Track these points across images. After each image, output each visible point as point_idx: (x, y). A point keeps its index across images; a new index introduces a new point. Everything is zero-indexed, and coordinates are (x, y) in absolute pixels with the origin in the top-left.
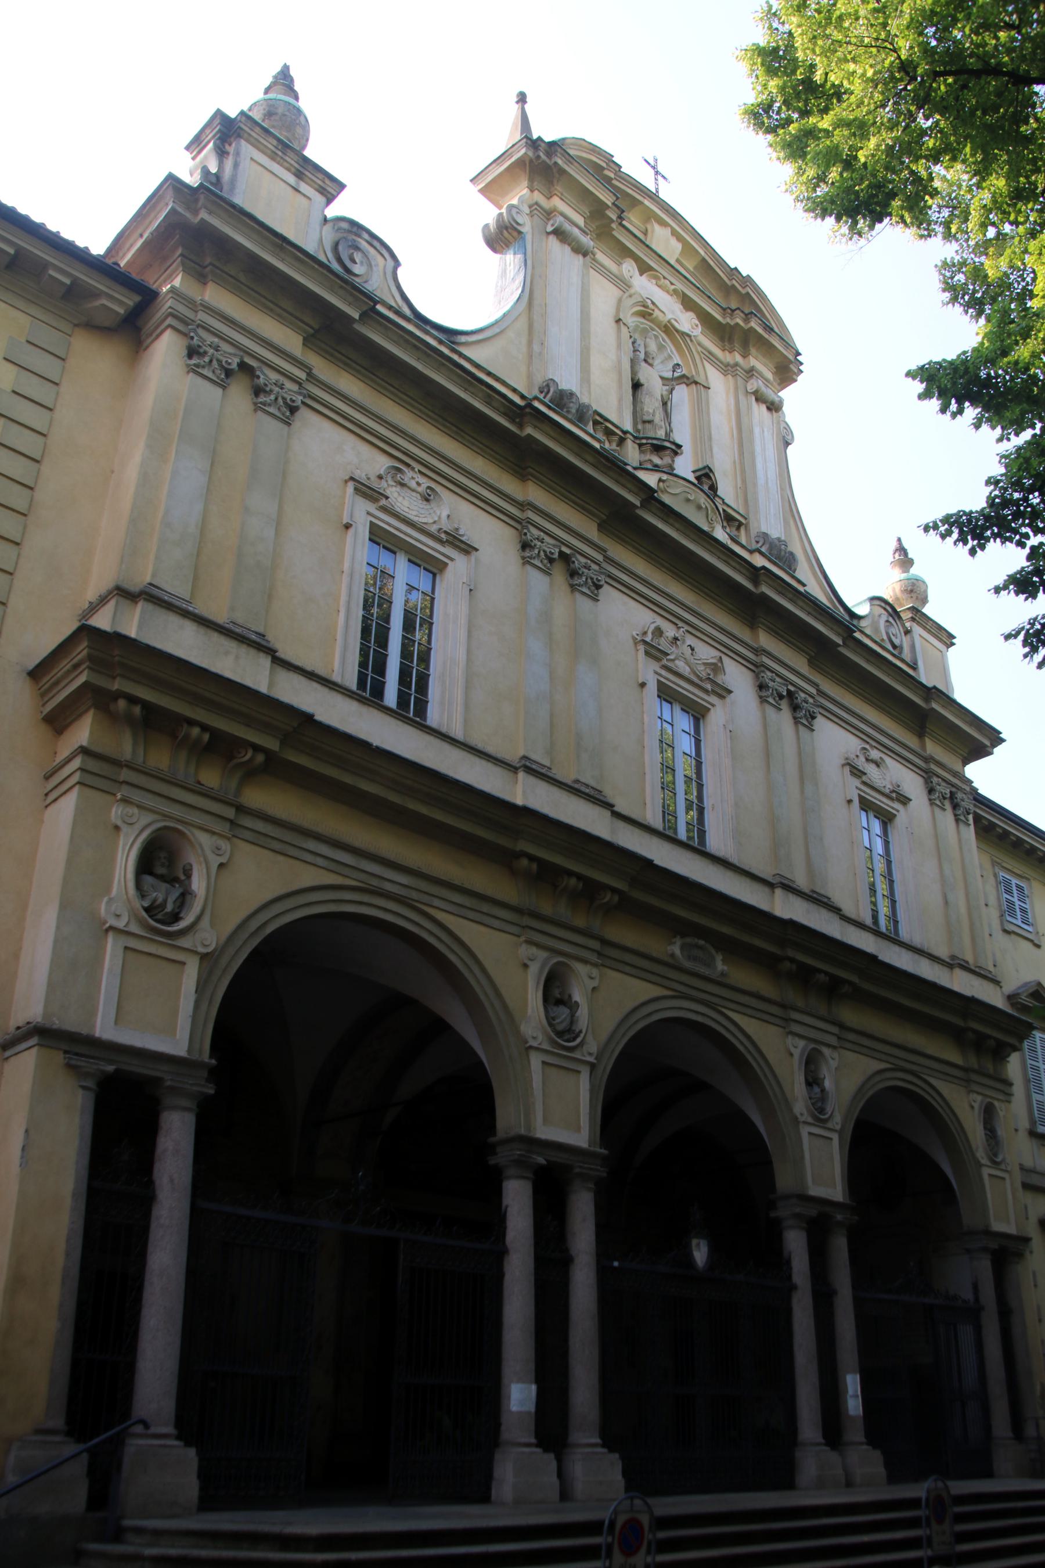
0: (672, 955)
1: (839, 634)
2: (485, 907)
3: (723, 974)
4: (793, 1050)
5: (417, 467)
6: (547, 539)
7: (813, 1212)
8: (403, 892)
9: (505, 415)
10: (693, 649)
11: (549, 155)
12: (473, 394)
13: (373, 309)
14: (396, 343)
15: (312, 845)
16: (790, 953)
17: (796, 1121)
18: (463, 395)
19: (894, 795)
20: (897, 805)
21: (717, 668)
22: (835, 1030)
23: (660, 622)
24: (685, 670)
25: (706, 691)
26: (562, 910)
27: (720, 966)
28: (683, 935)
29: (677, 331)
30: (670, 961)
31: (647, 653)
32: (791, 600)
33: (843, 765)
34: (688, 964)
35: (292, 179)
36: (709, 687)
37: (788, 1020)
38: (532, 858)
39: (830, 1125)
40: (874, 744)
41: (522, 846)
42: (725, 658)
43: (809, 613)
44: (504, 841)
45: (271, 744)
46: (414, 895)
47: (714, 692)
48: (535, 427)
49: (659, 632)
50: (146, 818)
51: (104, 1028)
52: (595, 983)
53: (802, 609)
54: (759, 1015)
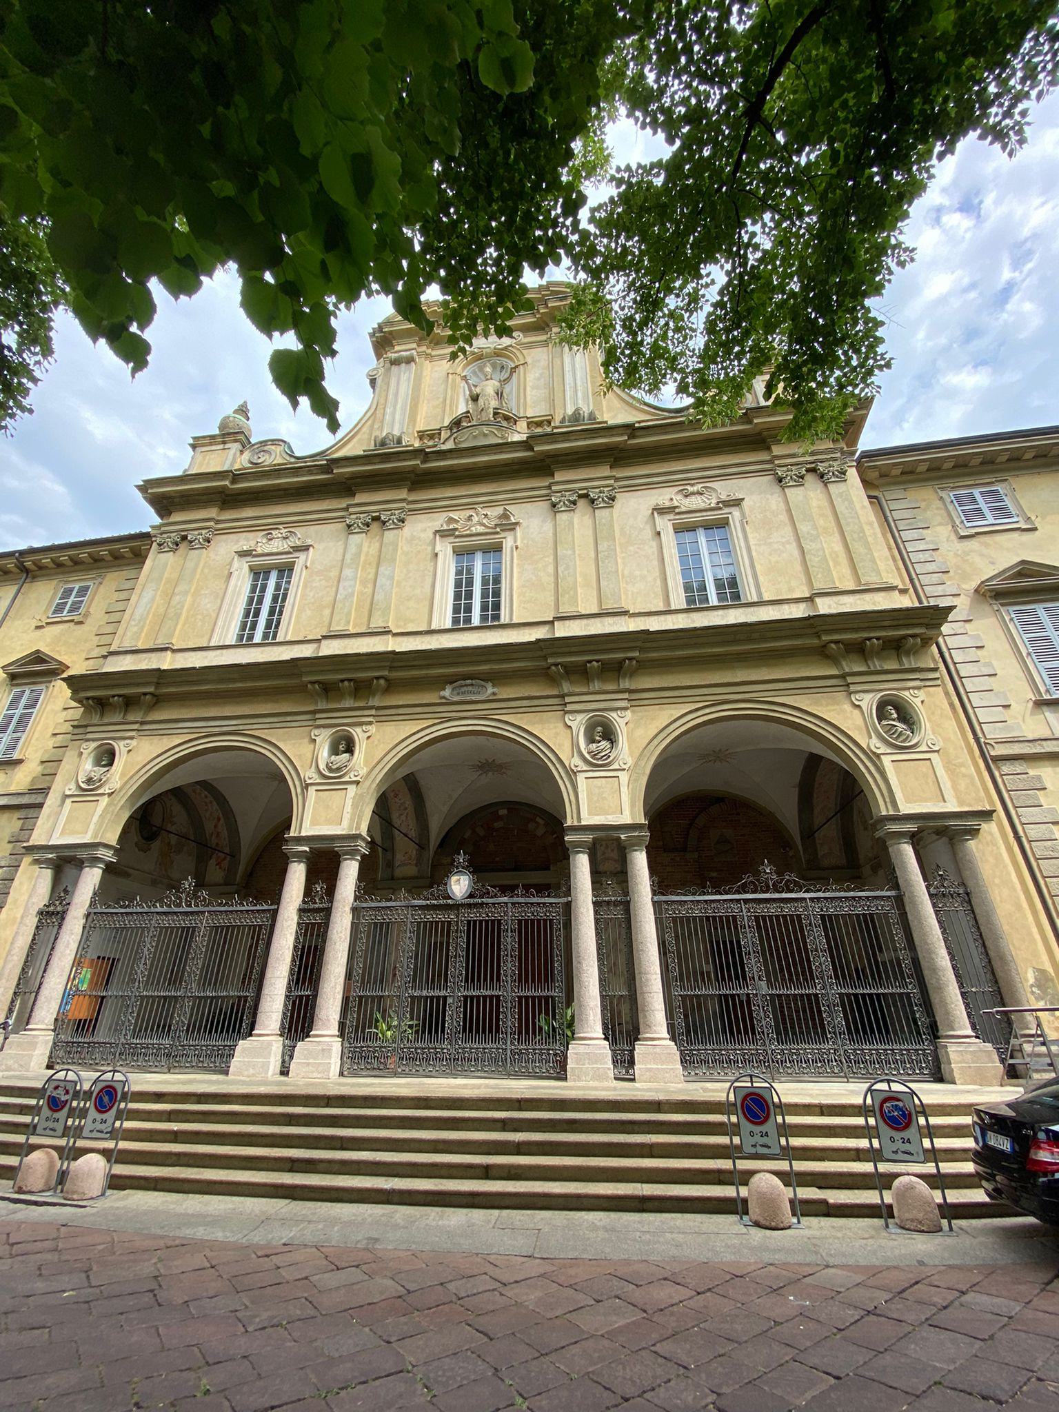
0: (444, 697)
1: (622, 435)
2: (289, 719)
3: (494, 694)
4: (569, 723)
5: (281, 527)
6: (362, 516)
7: (588, 837)
8: (234, 728)
9: (322, 473)
10: (486, 515)
11: (382, 332)
12: (303, 475)
13: (235, 475)
14: (255, 480)
15: (180, 725)
16: (550, 661)
17: (572, 774)
18: (295, 480)
19: (721, 505)
20: (726, 510)
21: (505, 516)
22: (626, 696)
23: (455, 515)
24: (480, 529)
25: (497, 533)
26: (348, 703)
27: (490, 690)
28: (451, 683)
29: (502, 349)
30: (444, 701)
31: (442, 536)
32: (563, 441)
33: (653, 513)
34: (457, 699)
35: (221, 446)
36: (498, 530)
37: (565, 704)
38: (313, 683)
39: (615, 766)
40: (693, 482)
41: (306, 679)
42: (507, 507)
43: (585, 439)
44: (294, 682)
45: (151, 689)
46: (241, 728)
47: (503, 530)
48: (338, 467)
49: (451, 520)
50: (94, 745)
51: (54, 841)
52: (368, 734)
53: (576, 440)
54: (533, 709)
